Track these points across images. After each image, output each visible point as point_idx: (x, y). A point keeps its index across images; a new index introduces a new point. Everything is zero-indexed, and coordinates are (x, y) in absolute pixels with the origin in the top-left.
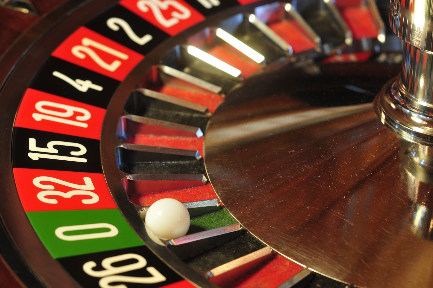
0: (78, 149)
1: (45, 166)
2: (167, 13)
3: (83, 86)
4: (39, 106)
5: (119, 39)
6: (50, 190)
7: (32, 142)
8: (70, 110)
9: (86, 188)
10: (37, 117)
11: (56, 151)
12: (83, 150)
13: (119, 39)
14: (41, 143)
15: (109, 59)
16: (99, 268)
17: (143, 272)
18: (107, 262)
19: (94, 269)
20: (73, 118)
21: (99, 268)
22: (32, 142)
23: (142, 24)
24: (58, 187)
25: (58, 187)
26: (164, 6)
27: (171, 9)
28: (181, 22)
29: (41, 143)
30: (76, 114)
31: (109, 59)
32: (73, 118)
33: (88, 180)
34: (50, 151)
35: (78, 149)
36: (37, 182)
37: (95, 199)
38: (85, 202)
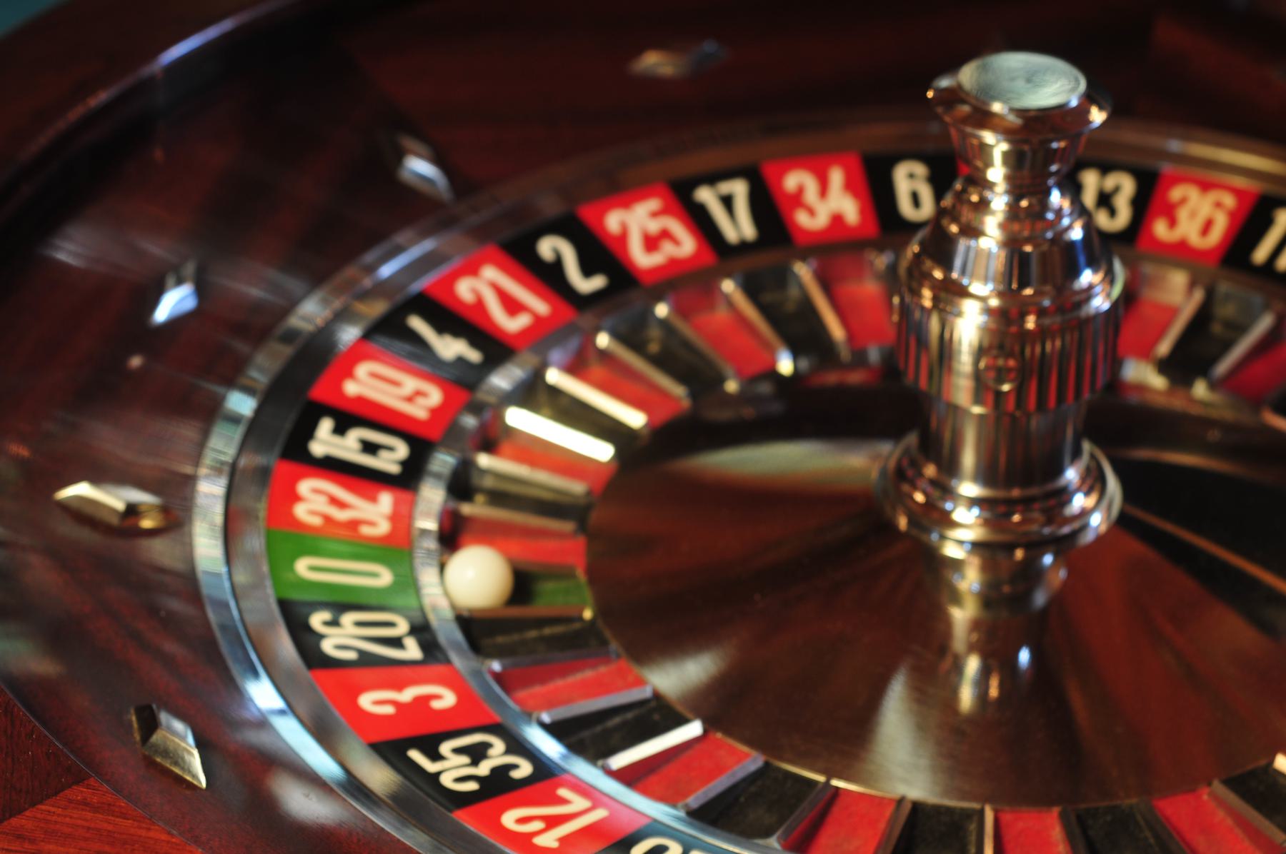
0: (390, 449)
1: (334, 467)
2: (651, 243)
3: (451, 348)
4: (363, 370)
5: (548, 277)
6: (321, 505)
7: (326, 426)
8: (410, 384)
9: (376, 512)
10: (351, 388)
11: (357, 446)
12: (402, 450)
13: (548, 277)
14: (340, 430)
15: (513, 306)
16: (334, 623)
17: (396, 643)
18: (348, 619)
19: (327, 624)
20: (410, 399)
21: (334, 623)
22: (326, 426)
23: (600, 253)
24: (335, 501)
25: (335, 501)
26: (654, 226)
27: (666, 234)
28: (673, 263)
29: (340, 430)
30: (419, 393)
31: (513, 306)
32: (410, 399)
33: (386, 500)
34: (348, 447)
35: (390, 449)
36: (306, 487)
37: (383, 528)
38: (366, 530)
